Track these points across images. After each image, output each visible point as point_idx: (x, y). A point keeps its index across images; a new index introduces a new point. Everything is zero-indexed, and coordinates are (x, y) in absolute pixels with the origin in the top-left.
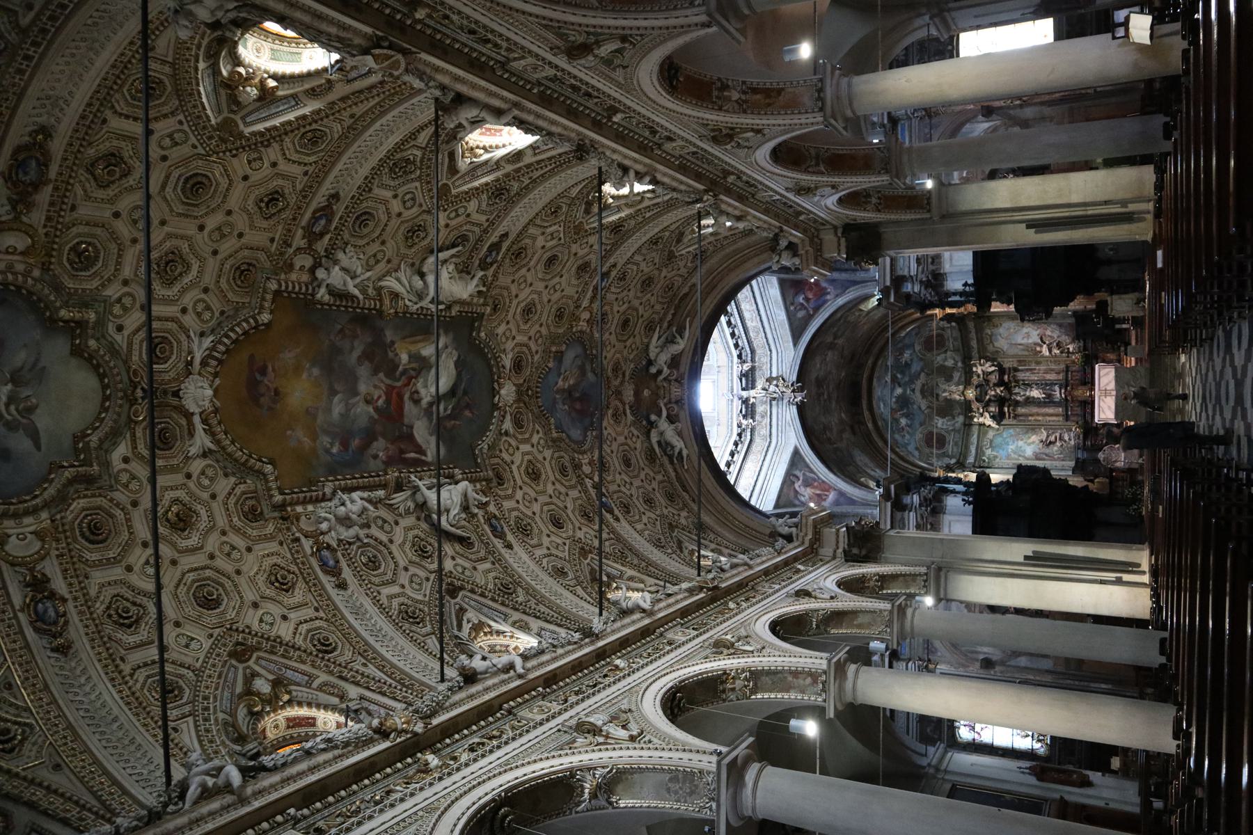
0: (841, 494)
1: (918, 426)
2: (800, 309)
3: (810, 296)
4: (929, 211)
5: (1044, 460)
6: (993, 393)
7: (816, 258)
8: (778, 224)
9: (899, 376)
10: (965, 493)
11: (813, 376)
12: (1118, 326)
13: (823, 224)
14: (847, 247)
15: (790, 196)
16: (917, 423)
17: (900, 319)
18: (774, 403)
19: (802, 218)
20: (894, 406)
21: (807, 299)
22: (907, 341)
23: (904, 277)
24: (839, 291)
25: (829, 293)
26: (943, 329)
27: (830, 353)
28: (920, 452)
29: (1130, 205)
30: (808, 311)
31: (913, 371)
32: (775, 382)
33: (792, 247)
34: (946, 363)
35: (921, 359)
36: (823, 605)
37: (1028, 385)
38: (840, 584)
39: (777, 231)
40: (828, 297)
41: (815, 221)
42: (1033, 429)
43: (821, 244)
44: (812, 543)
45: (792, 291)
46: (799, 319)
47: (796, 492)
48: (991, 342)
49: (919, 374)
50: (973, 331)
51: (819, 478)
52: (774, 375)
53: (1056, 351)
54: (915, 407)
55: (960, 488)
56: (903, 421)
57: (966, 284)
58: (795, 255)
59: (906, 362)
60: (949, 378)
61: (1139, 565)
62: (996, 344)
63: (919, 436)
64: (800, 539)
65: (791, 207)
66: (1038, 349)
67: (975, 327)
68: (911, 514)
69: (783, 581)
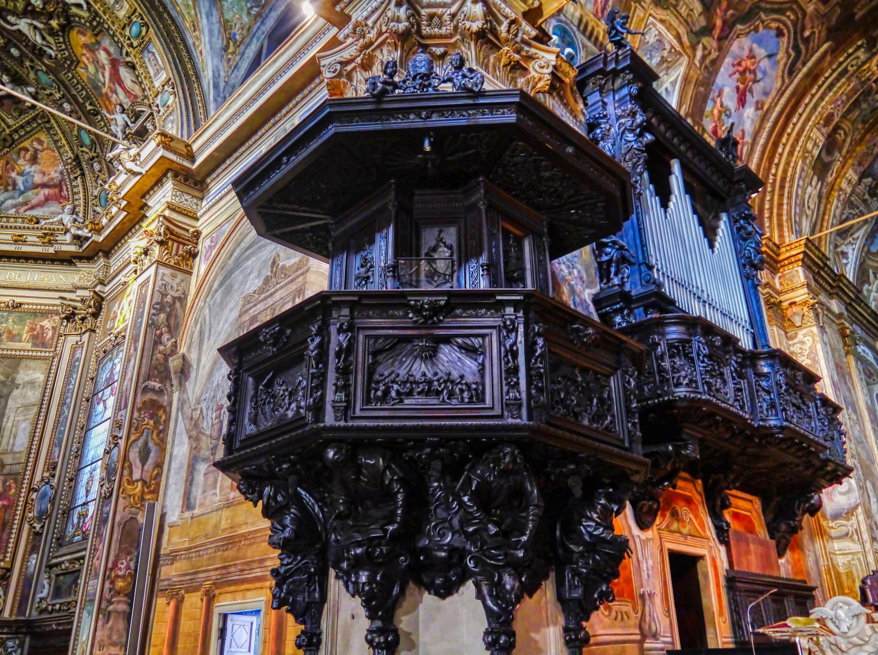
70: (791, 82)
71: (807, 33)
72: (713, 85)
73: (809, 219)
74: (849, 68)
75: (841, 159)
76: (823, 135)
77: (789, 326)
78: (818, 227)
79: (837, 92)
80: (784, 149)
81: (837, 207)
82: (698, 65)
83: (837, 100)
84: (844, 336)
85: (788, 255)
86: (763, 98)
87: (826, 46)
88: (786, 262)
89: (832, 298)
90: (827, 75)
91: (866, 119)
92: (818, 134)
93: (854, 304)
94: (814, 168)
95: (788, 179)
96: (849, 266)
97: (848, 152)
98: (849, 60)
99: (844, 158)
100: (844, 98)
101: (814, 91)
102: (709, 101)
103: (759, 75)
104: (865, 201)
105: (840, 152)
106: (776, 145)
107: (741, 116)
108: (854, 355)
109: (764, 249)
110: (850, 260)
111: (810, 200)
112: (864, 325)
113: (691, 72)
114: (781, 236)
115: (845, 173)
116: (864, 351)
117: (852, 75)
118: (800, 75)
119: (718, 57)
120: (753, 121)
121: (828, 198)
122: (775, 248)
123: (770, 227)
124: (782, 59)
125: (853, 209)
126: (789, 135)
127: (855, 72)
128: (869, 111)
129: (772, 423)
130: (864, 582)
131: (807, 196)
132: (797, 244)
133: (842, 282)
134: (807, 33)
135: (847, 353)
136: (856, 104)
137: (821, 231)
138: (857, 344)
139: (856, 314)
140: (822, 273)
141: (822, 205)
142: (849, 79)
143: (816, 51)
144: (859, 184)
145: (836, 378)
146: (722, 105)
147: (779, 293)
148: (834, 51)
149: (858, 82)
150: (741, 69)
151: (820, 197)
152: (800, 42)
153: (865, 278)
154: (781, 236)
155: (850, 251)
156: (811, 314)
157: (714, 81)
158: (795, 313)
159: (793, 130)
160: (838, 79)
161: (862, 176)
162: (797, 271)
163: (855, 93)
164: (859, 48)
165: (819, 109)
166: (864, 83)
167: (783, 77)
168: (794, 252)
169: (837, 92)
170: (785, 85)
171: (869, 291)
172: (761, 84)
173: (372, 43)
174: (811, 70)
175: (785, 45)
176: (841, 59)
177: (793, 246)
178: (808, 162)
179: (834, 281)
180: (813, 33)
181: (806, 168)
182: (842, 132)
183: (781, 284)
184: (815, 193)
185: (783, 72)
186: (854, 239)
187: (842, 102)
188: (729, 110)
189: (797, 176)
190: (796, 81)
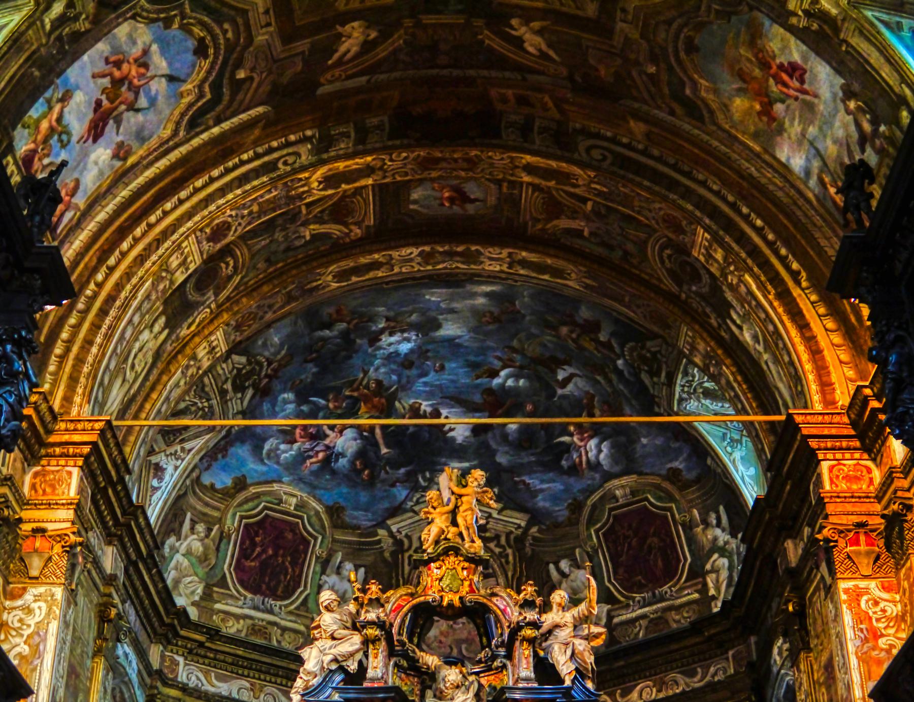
16: (339, 493)
17: (776, 280)
26: (698, 573)
28: (227, 494)
31: (533, 481)
35: (576, 507)
49: (521, 508)
50: (696, 683)
54: (401, 493)
59: (567, 448)
70: (188, 140)
71: (241, 75)
72: (59, 75)
73: (127, 386)
74: (280, 165)
75: (213, 306)
76: (202, 253)
77: (18, 572)
78: (134, 408)
79: (246, 193)
80: (132, 247)
81: (177, 385)
82: (48, 27)
83: (244, 206)
84: (103, 617)
85: (66, 438)
86: (135, 145)
87: (261, 109)
88: (58, 450)
89: (109, 543)
90: (245, 157)
91: (273, 259)
92: (195, 248)
93: (141, 566)
94: (166, 303)
95: (118, 303)
96: (159, 493)
97: (228, 299)
98: (285, 152)
99: (219, 306)
100: (255, 208)
101: (215, 173)
102: (41, 100)
103: (143, 102)
104: (223, 393)
105: (216, 295)
106: (123, 232)
107: (85, 155)
108: (106, 659)
109: (27, 411)
110: (163, 484)
111: (140, 356)
112: (144, 609)
113: (30, 32)
114: (68, 399)
115: (211, 334)
116: (126, 655)
117: (280, 177)
118: (205, 136)
119: (87, 31)
120: (101, 173)
121: (169, 363)
122: (48, 418)
123: (56, 374)
124: (189, 93)
125: (201, 398)
126: (150, 226)
127: (287, 174)
128: (282, 247)
131: (137, 345)
132: (89, 426)
133: (137, 521)
134: (241, 75)
135: (97, 652)
136: (269, 226)
137: (136, 417)
138: (119, 640)
139: (138, 583)
140: (110, 491)
141: (155, 372)
143: (244, 111)
144: (225, 361)
145: (61, 692)
146: (59, 120)
147: (24, 503)
149: (284, 193)
150: (117, 74)
151: (157, 355)
152: (225, 81)
153: (177, 525)
154: (68, 399)
155: (170, 469)
156: (64, 562)
157: (63, 71)
158: (36, 551)
159: (159, 221)
160: (257, 173)
161: (235, 348)
162: (70, 473)
163: (274, 210)
164: (306, 140)
165: (212, 207)
166: (291, 199)
167: (178, 123)
168: (76, 438)
169: (246, 193)
170: (176, 140)
171: (176, 551)
172: (140, 117)
174: (223, 135)
175: (202, 74)
176: (275, 144)
177: (80, 426)
178: (161, 287)
179: (123, 514)
180: (251, 79)
181: (153, 297)
182: (232, 263)
183: (33, 487)
184: (153, 345)
185: (182, 115)
186: (183, 449)
187: (251, 213)
188: (69, 134)
189: (135, 304)
190: (196, 142)
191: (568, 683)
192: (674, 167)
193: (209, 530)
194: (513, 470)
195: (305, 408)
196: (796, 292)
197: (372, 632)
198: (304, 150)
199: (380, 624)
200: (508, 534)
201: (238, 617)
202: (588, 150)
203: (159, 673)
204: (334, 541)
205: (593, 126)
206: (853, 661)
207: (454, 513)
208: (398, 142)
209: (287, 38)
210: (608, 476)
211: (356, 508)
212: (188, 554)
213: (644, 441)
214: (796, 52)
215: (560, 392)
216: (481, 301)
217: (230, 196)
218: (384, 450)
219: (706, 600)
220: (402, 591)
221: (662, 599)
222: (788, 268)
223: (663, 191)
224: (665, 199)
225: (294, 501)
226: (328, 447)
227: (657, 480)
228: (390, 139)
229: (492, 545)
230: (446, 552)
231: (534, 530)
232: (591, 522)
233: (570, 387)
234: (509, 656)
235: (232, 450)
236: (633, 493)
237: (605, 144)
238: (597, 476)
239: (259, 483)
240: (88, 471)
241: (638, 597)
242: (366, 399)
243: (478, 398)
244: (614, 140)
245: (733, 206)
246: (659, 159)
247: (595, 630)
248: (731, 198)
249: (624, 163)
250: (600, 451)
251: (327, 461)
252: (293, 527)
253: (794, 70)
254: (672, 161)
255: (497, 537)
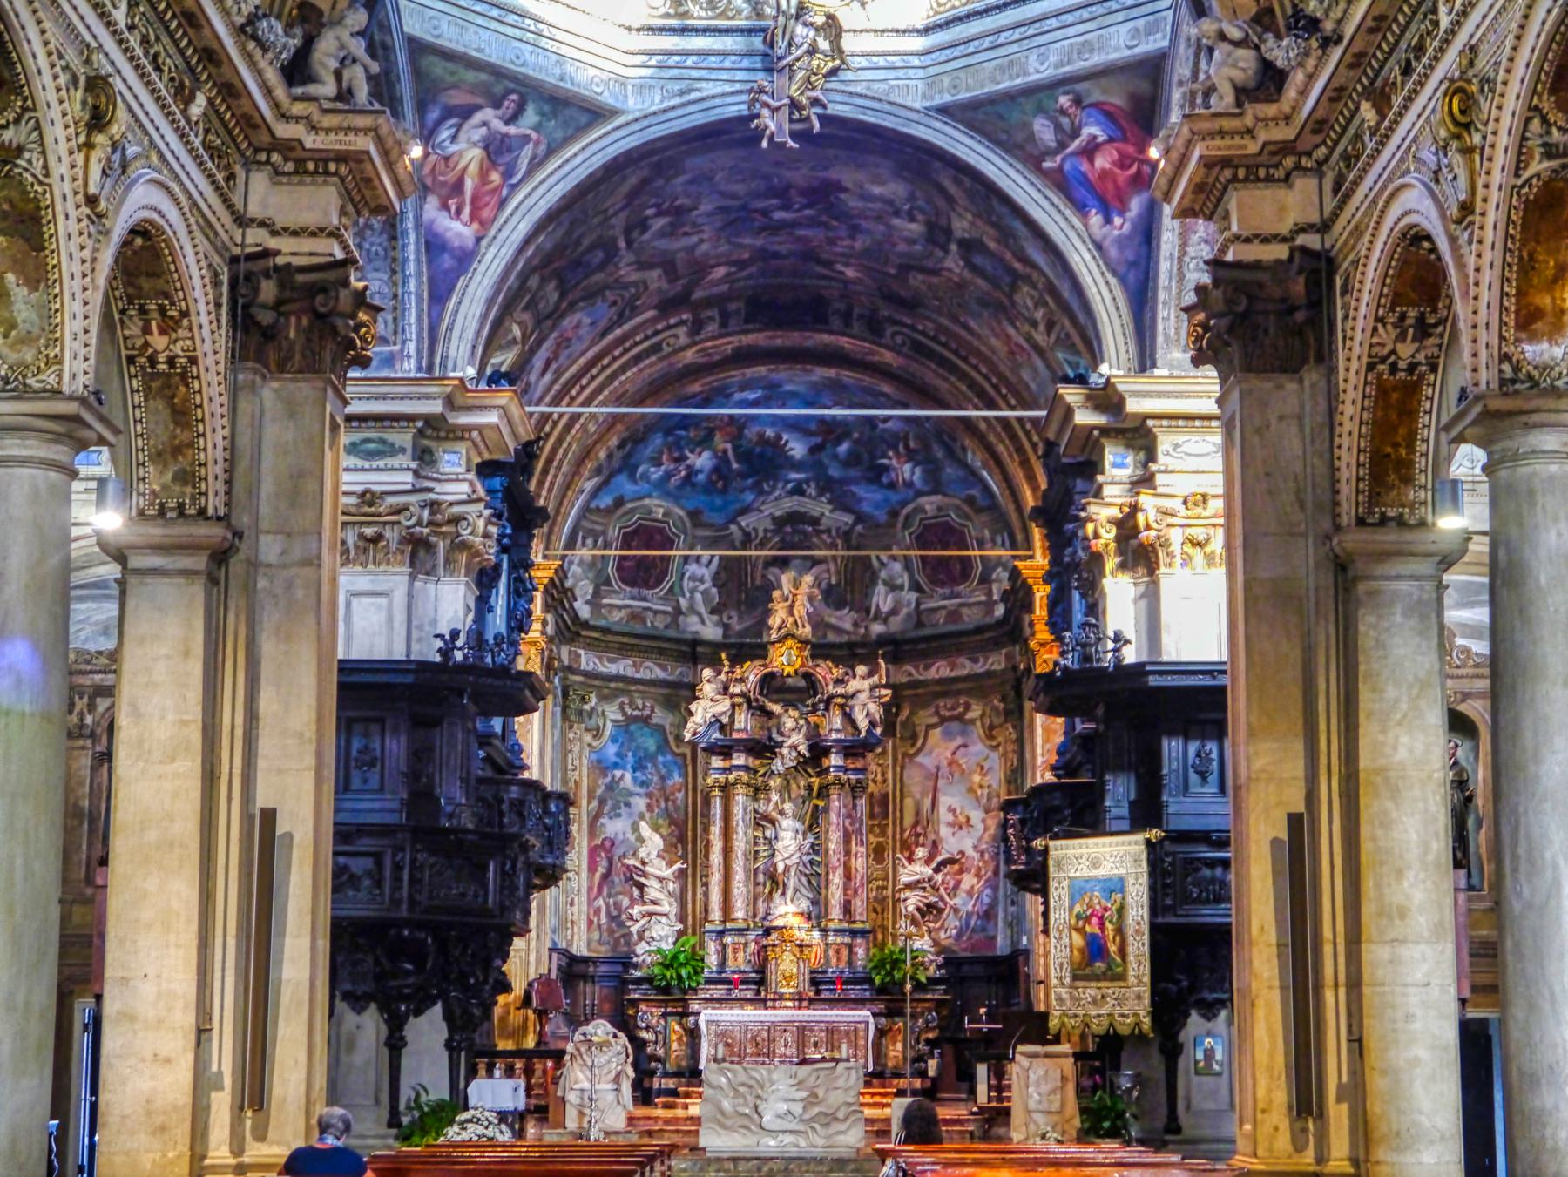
0: (466, 259)
1: (691, 505)
2: (1058, 128)
3: (1102, 162)
4: (1361, 522)
5: (592, 868)
6: (789, 723)
7: (1226, 162)
8: (1349, 30)
9: (844, 448)
10: (478, 638)
11: (847, 175)
12: (982, 1070)
13: (1336, 188)
14: (1257, 265)
15: (1449, 62)
16: (697, 501)
17: (1020, 450)
18: (757, 42)
19: (1368, 112)
20: (751, 433)
21: (1090, 150)
22: (950, 471)
23: (1151, 457)
24: (1113, 253)
25: (1108, 220)
26: (985, 580)
27: (915, 228)
28: (609, 511)
29: (1345, 1107)
30: (1055, 152)
31: (860, 491)
32: (824, 44)
33: (1270, 79)
34: (881, 588)
36: (60, 169)
37: (813, 822)
38: (145, 235)
39: (1328, 26)
40: (1095, 219)
41: (1349, 159)
42: (682, 839)
43: (1269, 179)
44: (288, 147)
45: (1117, 99)
46: (1027, 126)
47: (466, 113)
48: (943, 720)
49: (847, 509)
50: (979, 668)
51: (514, 187)
52: (848, 43)
53: (912, 901)
55: (498, 621)
56: (702, 461)
57: (1118, 638)
58: (1243, 94)
59: (886, 469)
60: (833, 596)
61: (261, 1135)
62: (936, 734)
63: (658, 507)
64: (298, 109)
65: (1407, 71)
66: (921, 852)
67: (989, 674)
68: (409, 477)
69: (145, 41)
90: (638, 338)
95: (555, 464)
129: (549, 860)
130: (530, 984)
142: (661, 359)
148: (653, 321)
164: (683, 323)
165: (616, 383)
169: (641, 370)
173: (379, 515)
176: (659, 327)
191: (863, 734)
192: (956, 353)
193: (596, 542)
194: (843, 482)
195: (670, 439)
196: (1033, 458)
197: (737, 700)
198: (682, 331)
199: (743, 695)
200: (838, 529)
201: (620, 608)
202: (894, 334)
203: (570, 669)
204: (694, 537)
205: (897, 317)
206: (1039, 731)
207: (791, 607)
208: (751, 326)
209: (671, 282)
210: (919, 494)
211: (712, 509)
212: (581, 563)
213: (949, 470)
214: (1025, 345)
215: (881, 426)
216: (814, 378)
217: (629, 374)
218: (735, 466)
219: (989, 605)
220: (757, 663)
221: (958, 596)
222: (1030, 440)
223: (946, 374)
224: (945, 379)
225: (661, 511)
226: (689, 467)
227: (957, 502)
228: (747, 321)
229: (824, 536)
230: (786, 637)
231: (859, 528)
232: (905, 526)
233: (889, 425)
234: (827, 709)
235: (614, 480)
236: (939, 509)
237: (905, 330)
238: (911, 493)
239: (632, 500)
240: (546, 591)
241: (940, 591)
242: (720, 428)
243: (813, 426)
244: (913, 328)
245: (996, 387)
246: (945, 345)
247: (884, 692)
248: (994, 380)
249: (918, 348)
250: (913, 473)
251: (688, 478)
252: (661, 531)
253: (1023, 349)
254: (954, 346)
255: (828, 531)
